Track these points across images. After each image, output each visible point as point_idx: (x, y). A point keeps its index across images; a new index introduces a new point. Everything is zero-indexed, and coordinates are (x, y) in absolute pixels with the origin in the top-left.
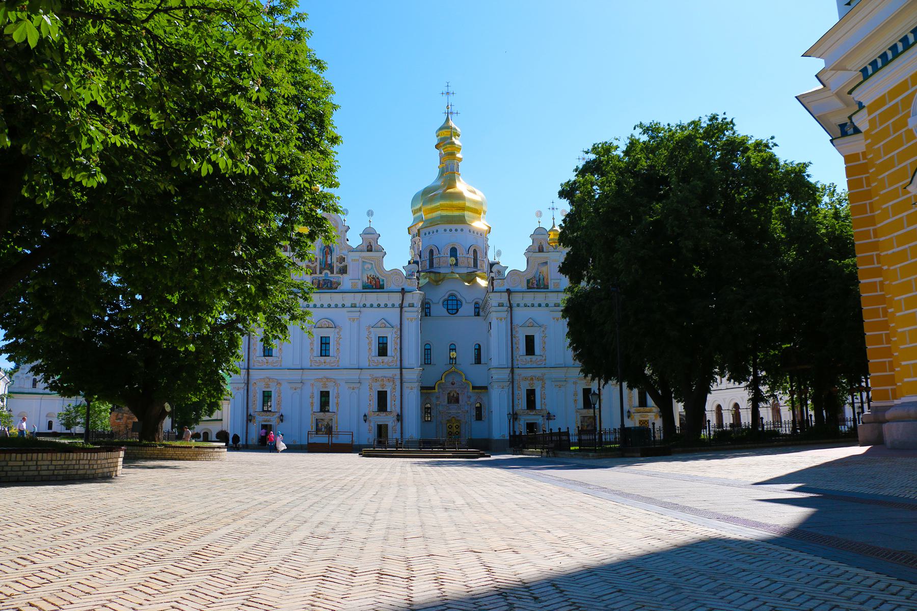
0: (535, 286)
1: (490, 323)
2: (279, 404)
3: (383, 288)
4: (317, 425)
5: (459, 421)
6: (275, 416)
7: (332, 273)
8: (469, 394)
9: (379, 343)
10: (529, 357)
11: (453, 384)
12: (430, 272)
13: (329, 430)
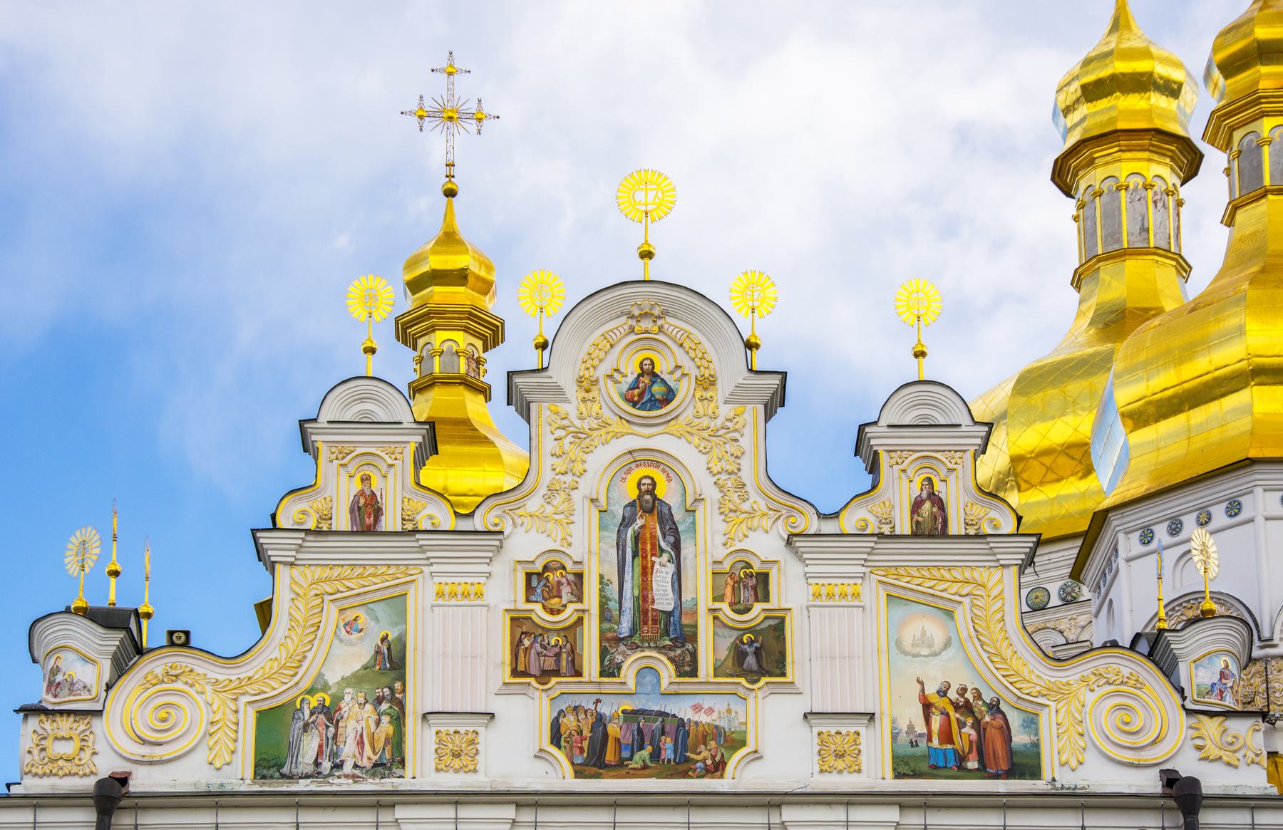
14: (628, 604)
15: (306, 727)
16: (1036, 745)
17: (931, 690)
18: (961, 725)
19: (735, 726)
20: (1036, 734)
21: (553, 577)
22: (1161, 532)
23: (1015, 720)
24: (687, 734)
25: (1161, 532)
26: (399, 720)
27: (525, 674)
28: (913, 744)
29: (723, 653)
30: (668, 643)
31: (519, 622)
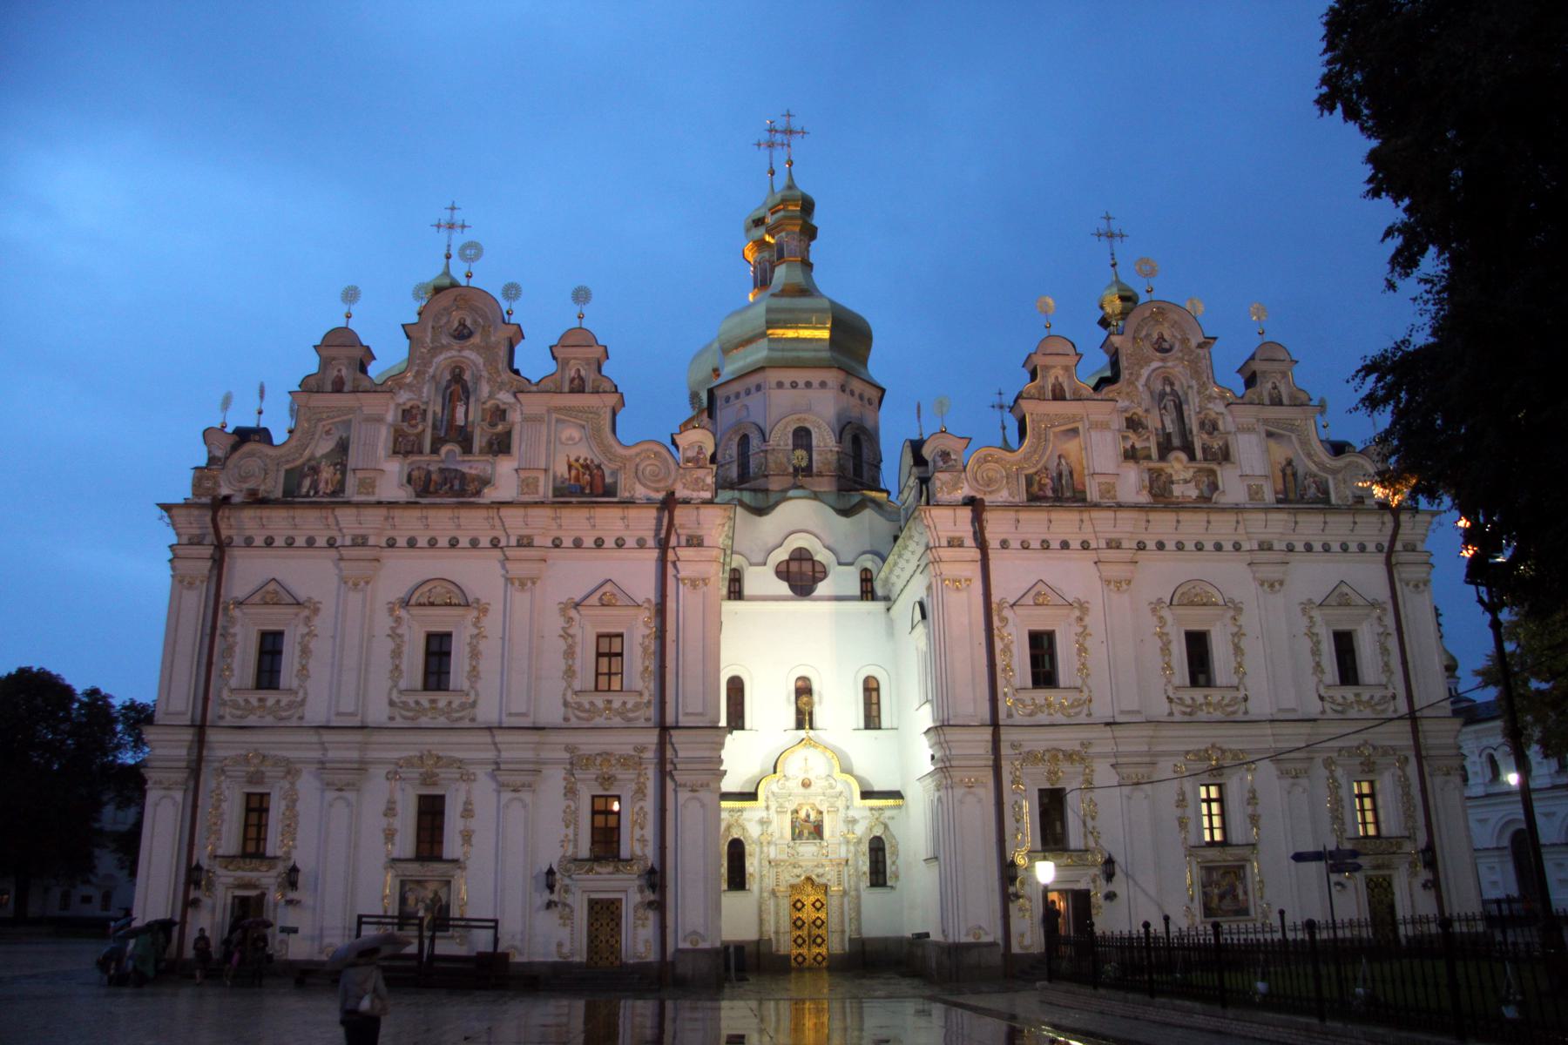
0: (1050, 493)
2: (290, 828)
3: (614, 495)
4: (403, 900)
6: (273, 873)
7: (467, 448)
8: (851, 813)
9: (599, 655)
10: (1041, 695)
11: (806, 784)
12: (741, 490)
13: (442, 919)
14: (444, 423)
15: (305, 476)
16: (616, 483)
18: (584, 474)
23: (607, 472)
24: (465, 478)
26: (344, 473)
28: (563, 482)
29: (484, 444)
30: (460, 439)
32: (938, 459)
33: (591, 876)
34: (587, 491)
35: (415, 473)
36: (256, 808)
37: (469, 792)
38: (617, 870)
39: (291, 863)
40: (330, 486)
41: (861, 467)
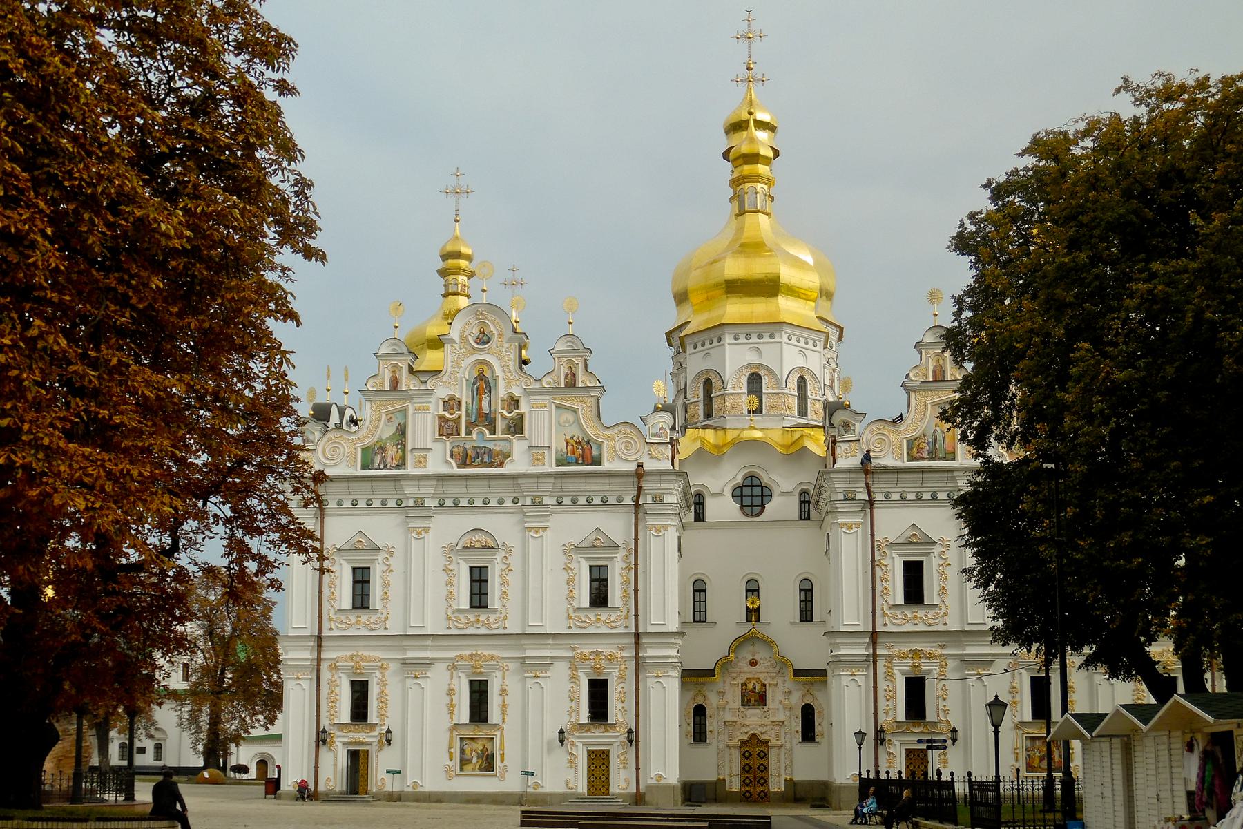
1: (828, 534)
4: (463, 751)
5: (767, 742)
6: (376, 733)
9: (592, 580)
11: (753, 663)
12: (705, 427)
14: (474, 411)
15: (376, 454)
16: (600, 455)
17: (568, 437)
19: (507, 451)
20: (601, 451)
21: (452, 403)
22: (699, 345)
23: (594, 447)
25: (699, 345)
26: (404, 451)
27: (443, 435)
28: (562, 455)
31: (441, 418)
32: (841, 428)
33: (589, 734)
34: (580, 462)
35: (456, 450)
36: (360, 691)
37: (504, 679)
38: (607, 730)
39: (386, 728)
40: (394, 461)
41: (806, 403)
